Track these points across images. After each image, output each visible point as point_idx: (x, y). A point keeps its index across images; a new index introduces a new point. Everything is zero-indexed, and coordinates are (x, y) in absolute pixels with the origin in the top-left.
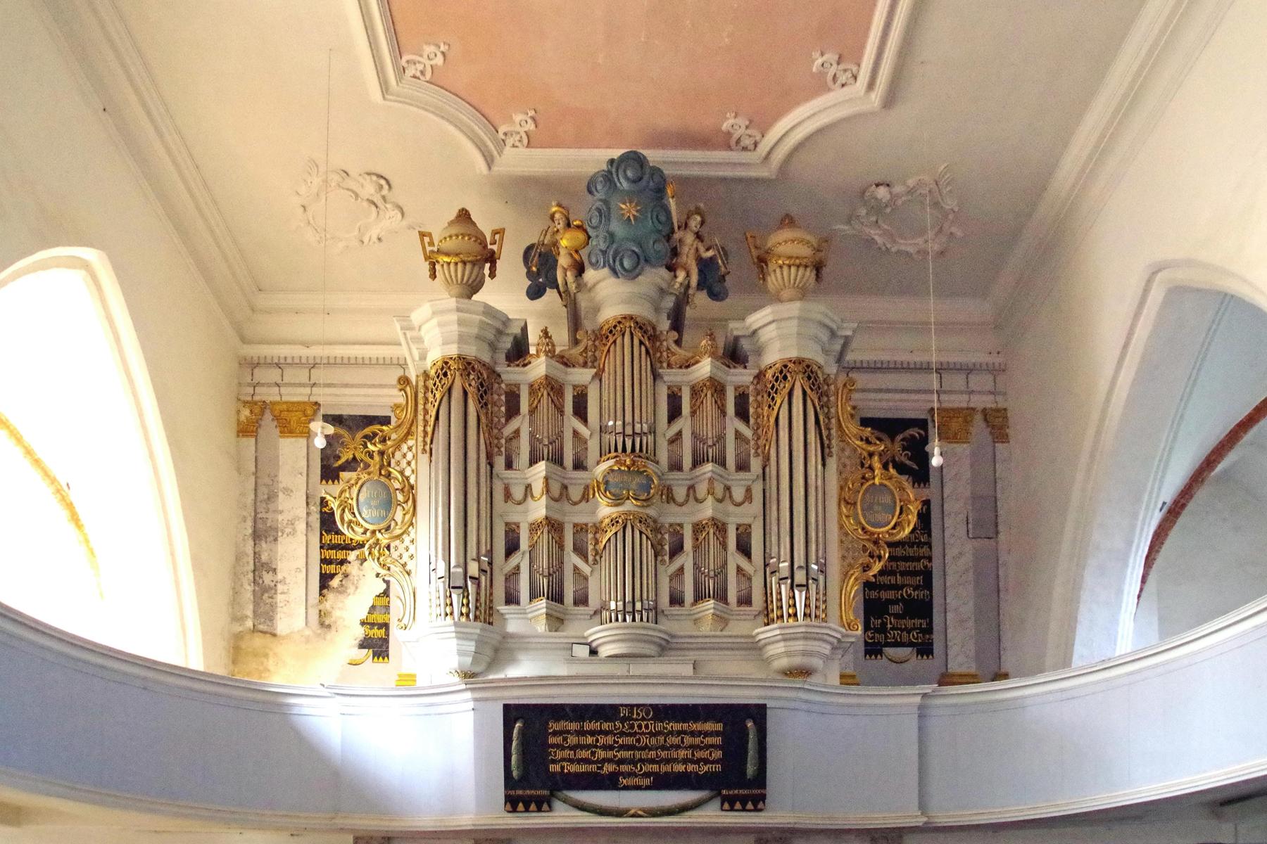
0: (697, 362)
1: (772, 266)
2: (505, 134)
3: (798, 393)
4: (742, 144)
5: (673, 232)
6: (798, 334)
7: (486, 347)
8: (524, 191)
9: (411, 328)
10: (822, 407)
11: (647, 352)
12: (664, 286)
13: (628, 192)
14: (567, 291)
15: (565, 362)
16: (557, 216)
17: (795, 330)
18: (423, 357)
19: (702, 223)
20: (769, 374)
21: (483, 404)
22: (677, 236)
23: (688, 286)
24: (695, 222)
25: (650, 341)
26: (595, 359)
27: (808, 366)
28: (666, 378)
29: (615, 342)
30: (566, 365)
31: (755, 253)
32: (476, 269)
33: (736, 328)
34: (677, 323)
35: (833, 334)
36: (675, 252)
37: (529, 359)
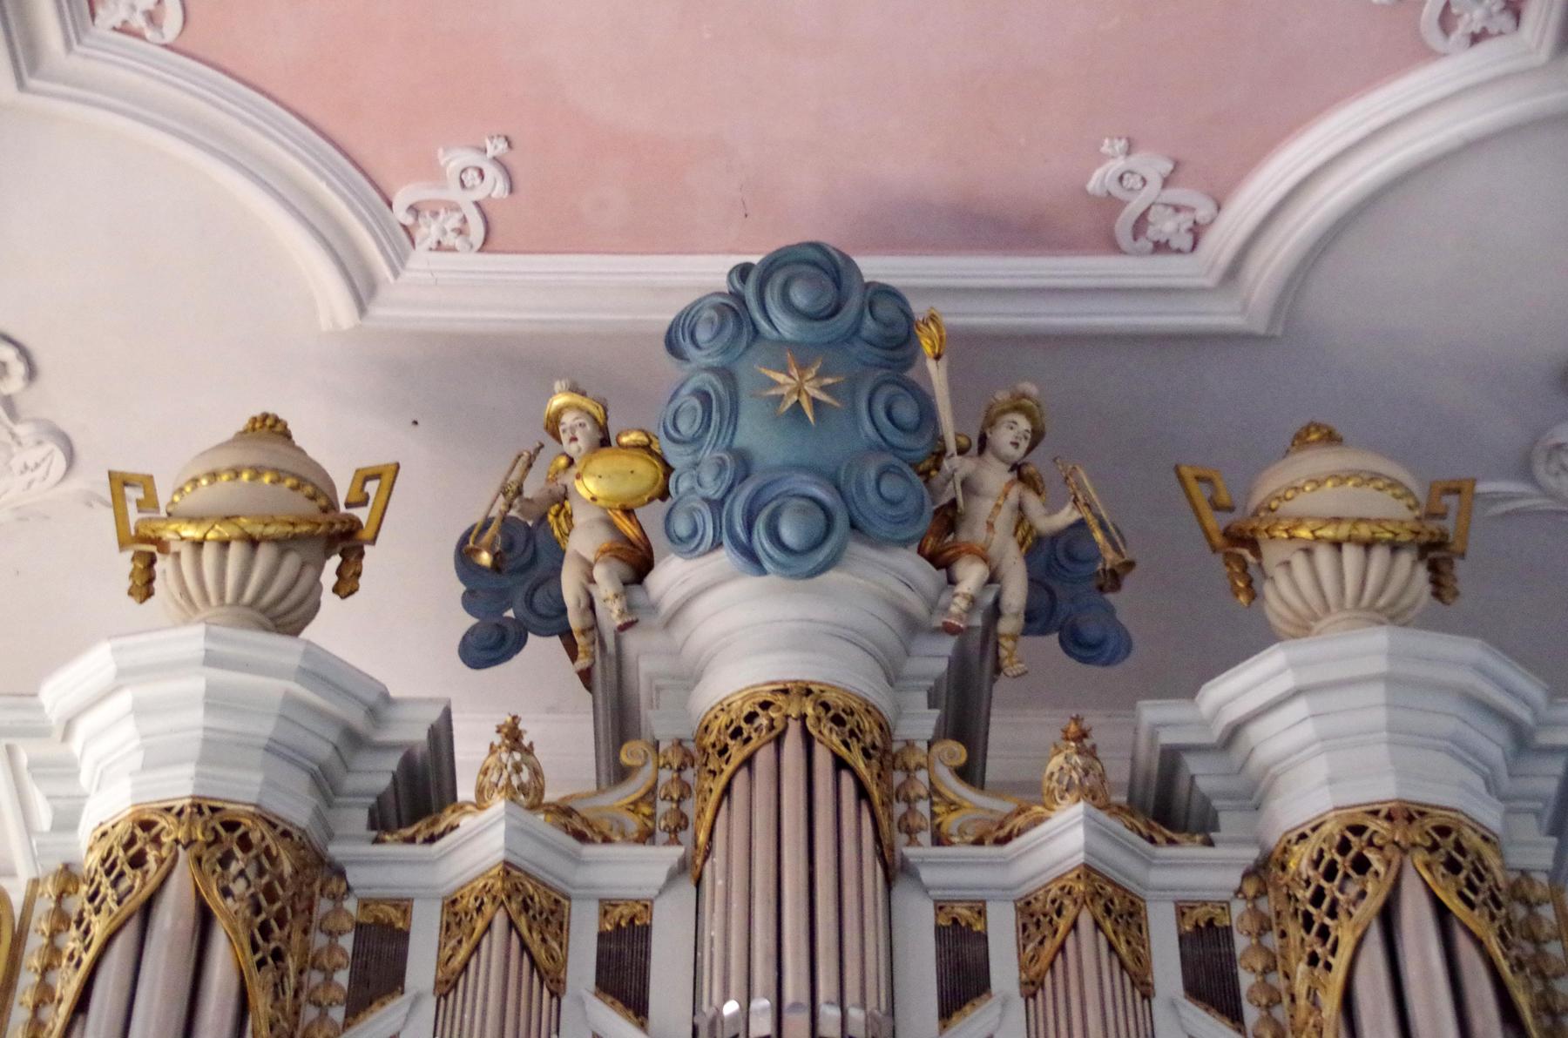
0: (1039, 820)
1: (1273, 554)
2: (414, 209)
3: (1416, 918)
4: (1152, 232)
5: (940, 454)
6: (1391, 728)
7: (301, 782)
8: (460, 374)
9: (38, 732)
10: (1518, 965)
11: (862, 793)
12: (917, 606)
13: (793, 346)
14: (593, 627)
15: (580, 827)
16: (568, 419)
17: (1380, 717)
18: (66, 822)
19: (1037, 437)
20: (1301, 860)
21: (267, 943)
22: (957, 465)
23: (995, 612)
24: (1010, 434)
25: (870, 767)
26: (680, 824)
27: (1444, 831)
28: (926, 875)
29: (748, 762)
30: (581, 837)
31: (1216, 522)
32: (291, 562)
33: (1164, 720)
34: (964, 716)
35: (1522, 740)
36: (949, 518)
37: (448, 818)
